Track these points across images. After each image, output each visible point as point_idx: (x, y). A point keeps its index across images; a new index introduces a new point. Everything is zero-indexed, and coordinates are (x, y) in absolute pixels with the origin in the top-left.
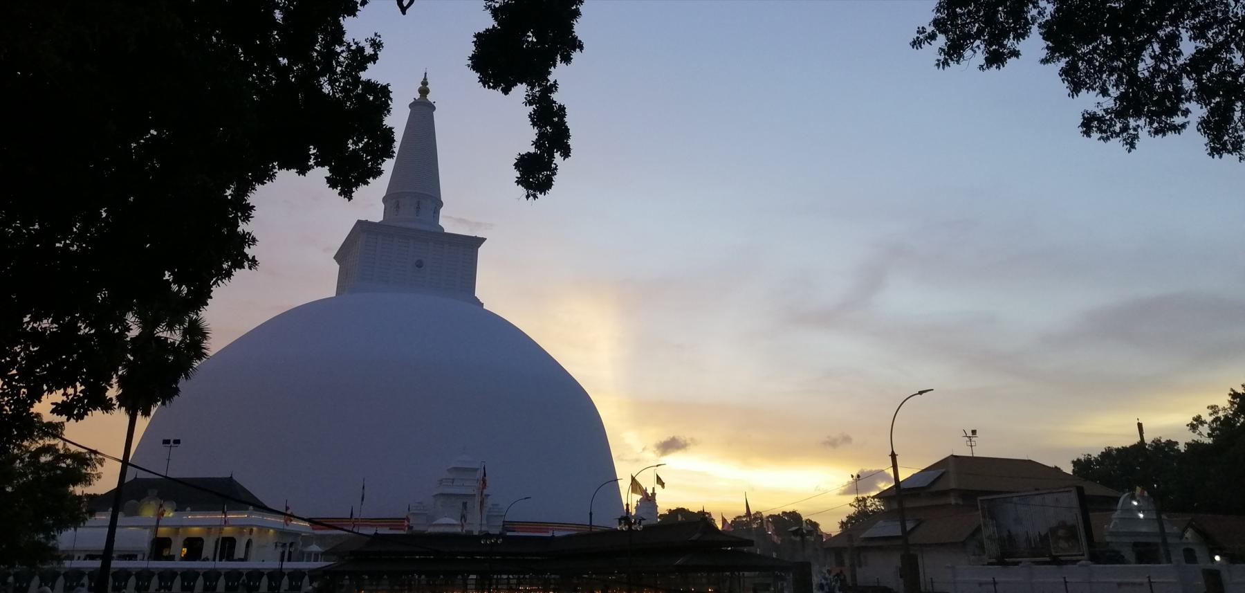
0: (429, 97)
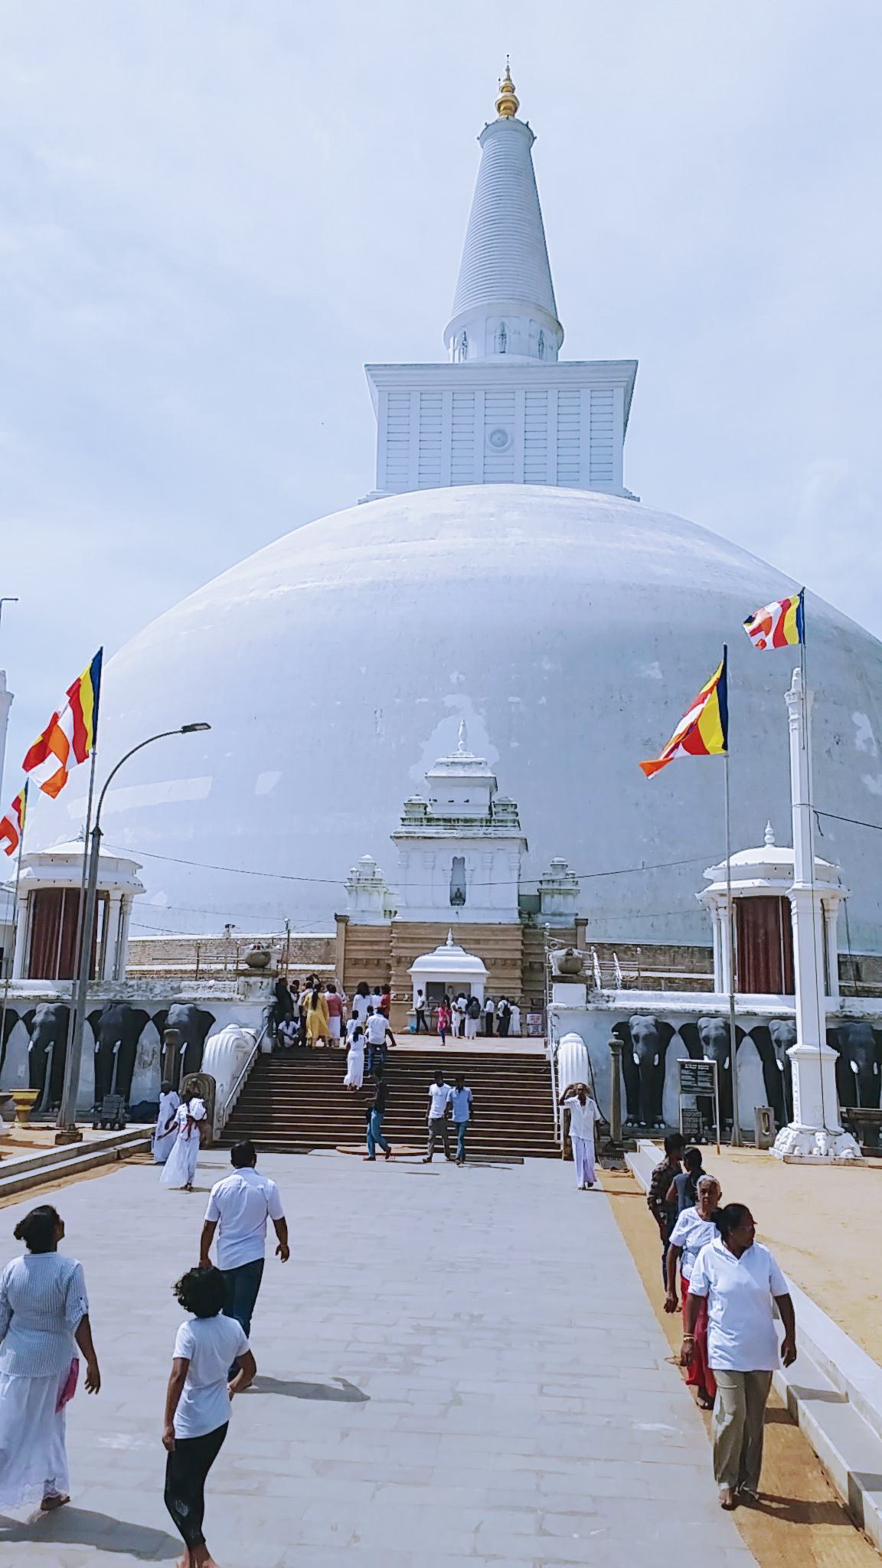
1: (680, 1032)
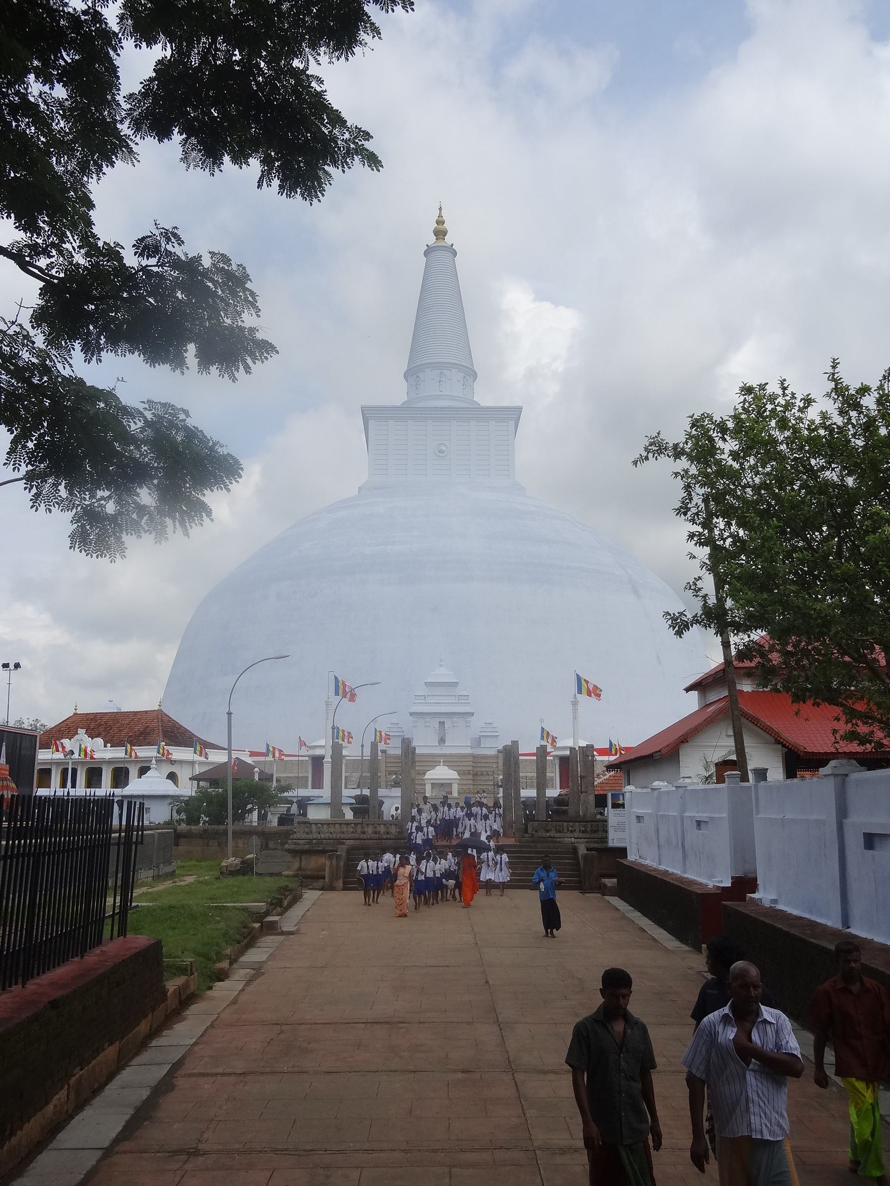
0: (449, 240)
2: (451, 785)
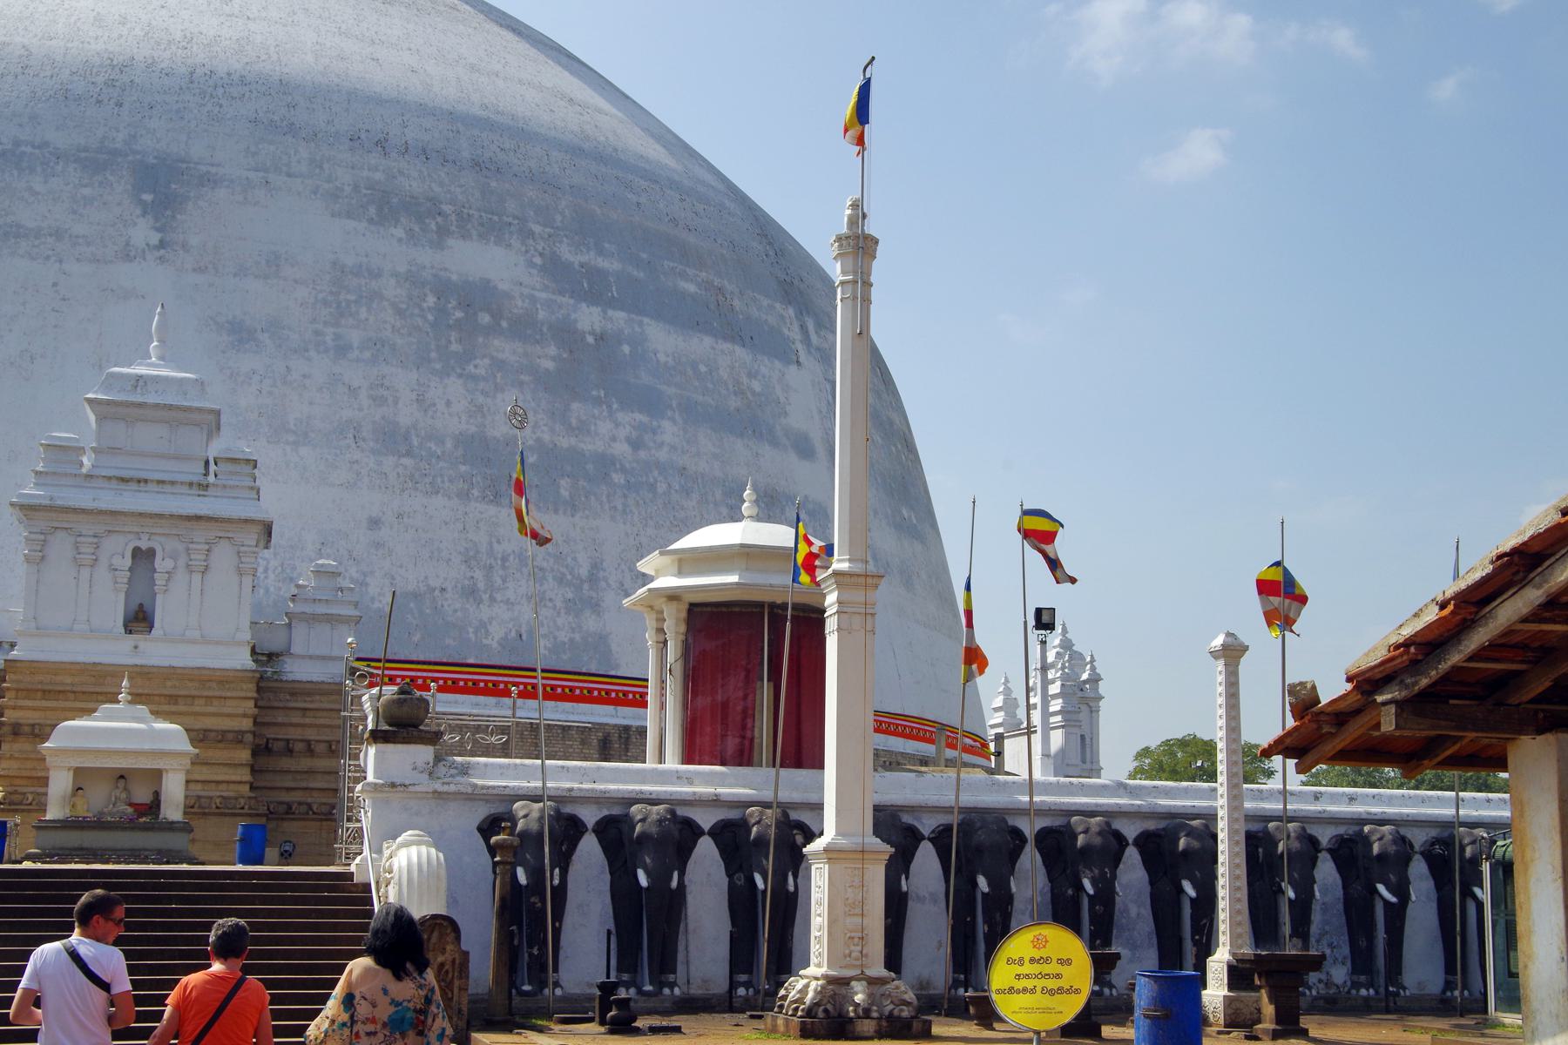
1: (587, 830)
2: (157, 775)
